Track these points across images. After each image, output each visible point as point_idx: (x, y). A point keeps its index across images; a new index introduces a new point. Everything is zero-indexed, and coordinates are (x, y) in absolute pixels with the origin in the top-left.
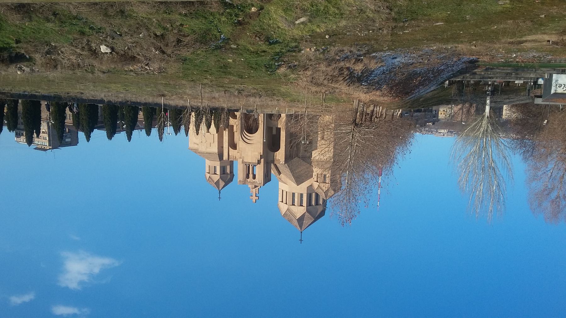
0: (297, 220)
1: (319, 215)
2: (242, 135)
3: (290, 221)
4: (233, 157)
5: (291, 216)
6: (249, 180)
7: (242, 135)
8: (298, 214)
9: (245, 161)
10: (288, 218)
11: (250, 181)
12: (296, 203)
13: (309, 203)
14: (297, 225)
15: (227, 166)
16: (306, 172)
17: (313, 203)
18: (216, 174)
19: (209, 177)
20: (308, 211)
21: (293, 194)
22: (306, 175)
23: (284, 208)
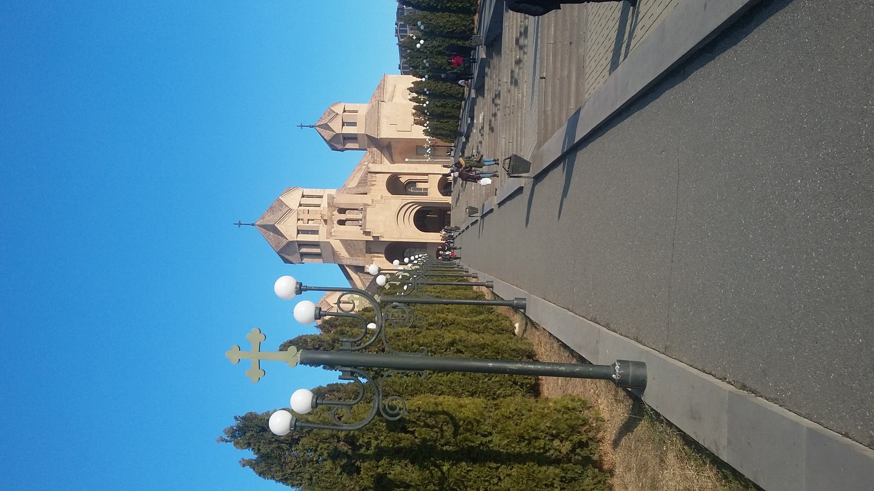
0: (274, 226)
2: (411, 204)
3: (270, 208)
4: (373, 181)
5: (280, 214)
6: (336, 213)
7: (411, 204)
10: (275, 207)
13: (302, 244)
14: (265, 219)
15: (357, 144)
17: (304, 250)
18: (343, 125)
20: (290, 243)
22: (350, 244)
23: (292, 199)
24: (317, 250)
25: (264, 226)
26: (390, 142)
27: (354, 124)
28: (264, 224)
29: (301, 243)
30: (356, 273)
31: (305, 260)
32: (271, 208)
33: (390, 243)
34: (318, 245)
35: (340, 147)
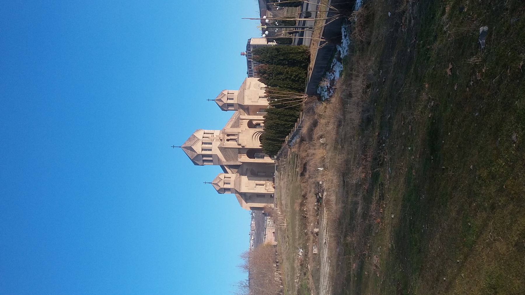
0: (191, 147)
1: (194, 162)
3: (188, 139)
6: (226, 136)
8: (195, 148)
9: (240, 134)
11: (225, 137)
12: (204, 145)
13: (204, 156)
14: (186, 144)
15: (233, 108)
16: (229, 156)
17: (204, 158)
19: (225, 95)
20: (198, 155)
21: (211, 144)
22: (227, 155)
24: (211, 159)
25: (185, 148)
27: (233, 99)
28: (186, 146)
30: (229, 169)
32: (189, 139)
33: (249, 149)
34: (211, 156)
35: (226, 109)
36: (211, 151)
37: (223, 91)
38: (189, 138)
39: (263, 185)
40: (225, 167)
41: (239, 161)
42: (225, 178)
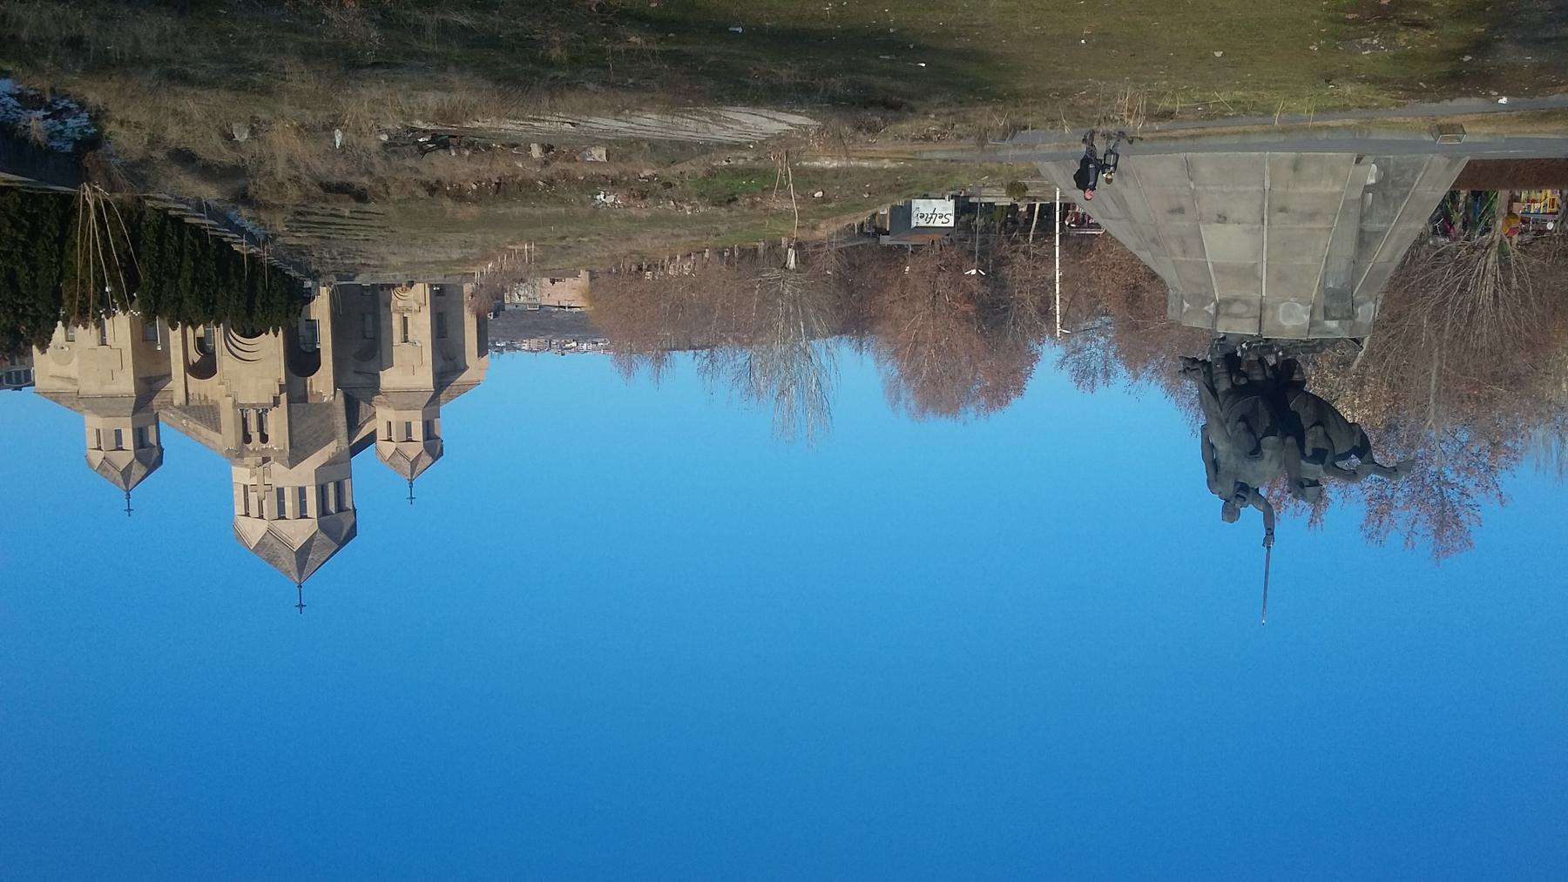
0: (296, 553)
1: (345, 538)
2: (229, 343)
6: (250, 446)
7: (229, 343)
10: (268, 555)
11: (254, 449)
12: (289, 512)
14: (290, 569)
15: (150, 427)
17: (332, 507)
21: (280, 492)
23: (254, 530)
25: (301, 569)
26: (141, 379)
27: (118, 433)
28: (296, 569)
29: (321, 513)
30: (360, 428)
31: (348, 505)
35: (156, 453)
36: (304, 488)
37: (90, 465)
38: (267, 560)
39: (405, 319)
40: (354, 442)
41: (332, 398)
42: (390, 440)
